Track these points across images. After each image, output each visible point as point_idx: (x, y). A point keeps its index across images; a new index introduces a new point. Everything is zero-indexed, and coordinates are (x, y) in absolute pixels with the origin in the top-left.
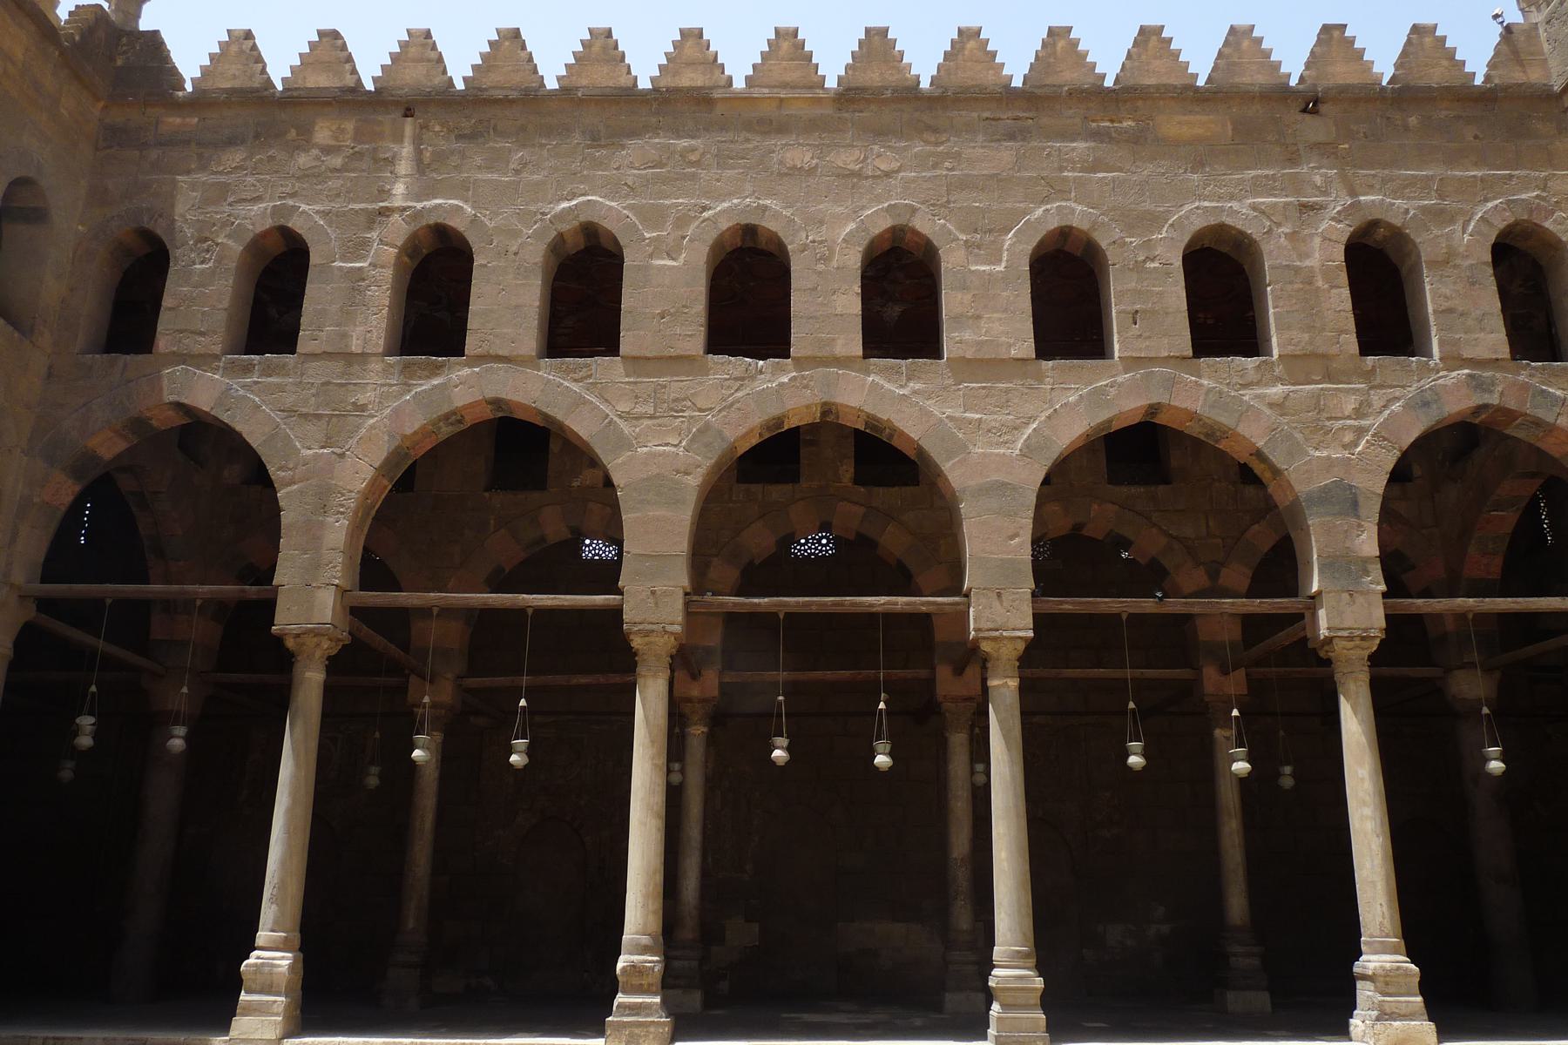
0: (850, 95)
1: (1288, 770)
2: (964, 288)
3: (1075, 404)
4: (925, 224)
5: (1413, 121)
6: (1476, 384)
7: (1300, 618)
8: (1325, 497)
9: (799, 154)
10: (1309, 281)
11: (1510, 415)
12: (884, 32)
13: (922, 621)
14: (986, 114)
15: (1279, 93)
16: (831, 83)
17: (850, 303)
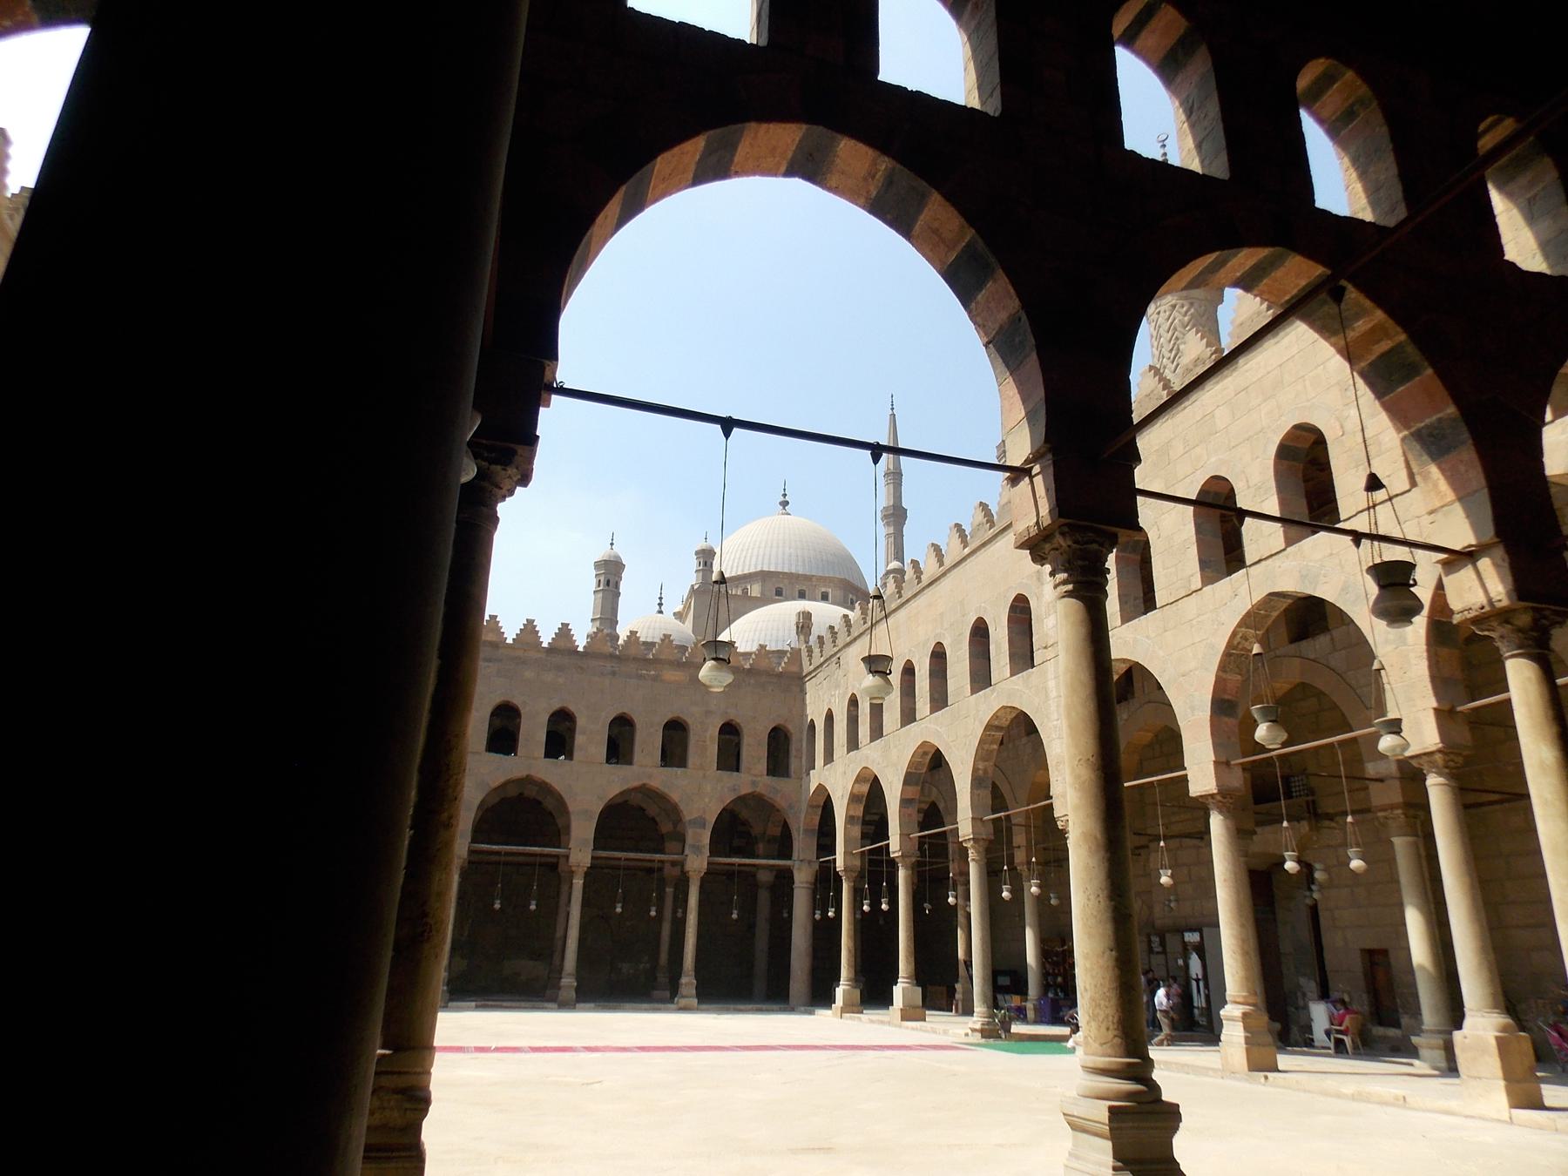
0: (552, 649)
3: (615, 781)
4: (572, 708)
6: (754, 783)
7: (682, 864)
8: (694, 822)
9: (528, 674)
16: (545, 645)
17: (542, 737)
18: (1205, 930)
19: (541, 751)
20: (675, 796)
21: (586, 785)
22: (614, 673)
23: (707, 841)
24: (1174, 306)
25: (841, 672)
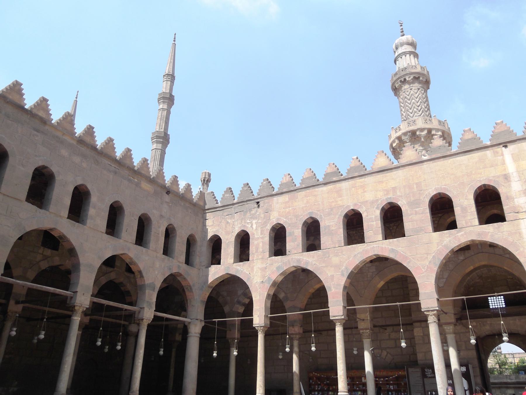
0: (81, 141)
1: (107, 347)
2: (94, 208)
3: (110, 247)
4: (89, 187)
5: (182, 204)
6: (179, 267)
9: (64, 152)
10: (158, 234)
11: (180, 275)
12: (93, 128)
13: (66, 297)
14: (109, 163)
15: (163, 187)
17: (68, 201)
18: (470, 367)
19: (65, 213)
20: (141, 266)
21: (92, 246)
22: (115, 173)
23: (154, 300)
24: (419, 89)
25: (259, 210)
